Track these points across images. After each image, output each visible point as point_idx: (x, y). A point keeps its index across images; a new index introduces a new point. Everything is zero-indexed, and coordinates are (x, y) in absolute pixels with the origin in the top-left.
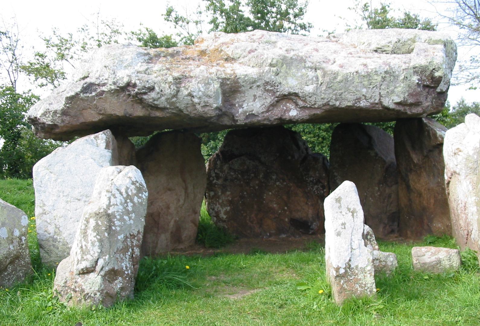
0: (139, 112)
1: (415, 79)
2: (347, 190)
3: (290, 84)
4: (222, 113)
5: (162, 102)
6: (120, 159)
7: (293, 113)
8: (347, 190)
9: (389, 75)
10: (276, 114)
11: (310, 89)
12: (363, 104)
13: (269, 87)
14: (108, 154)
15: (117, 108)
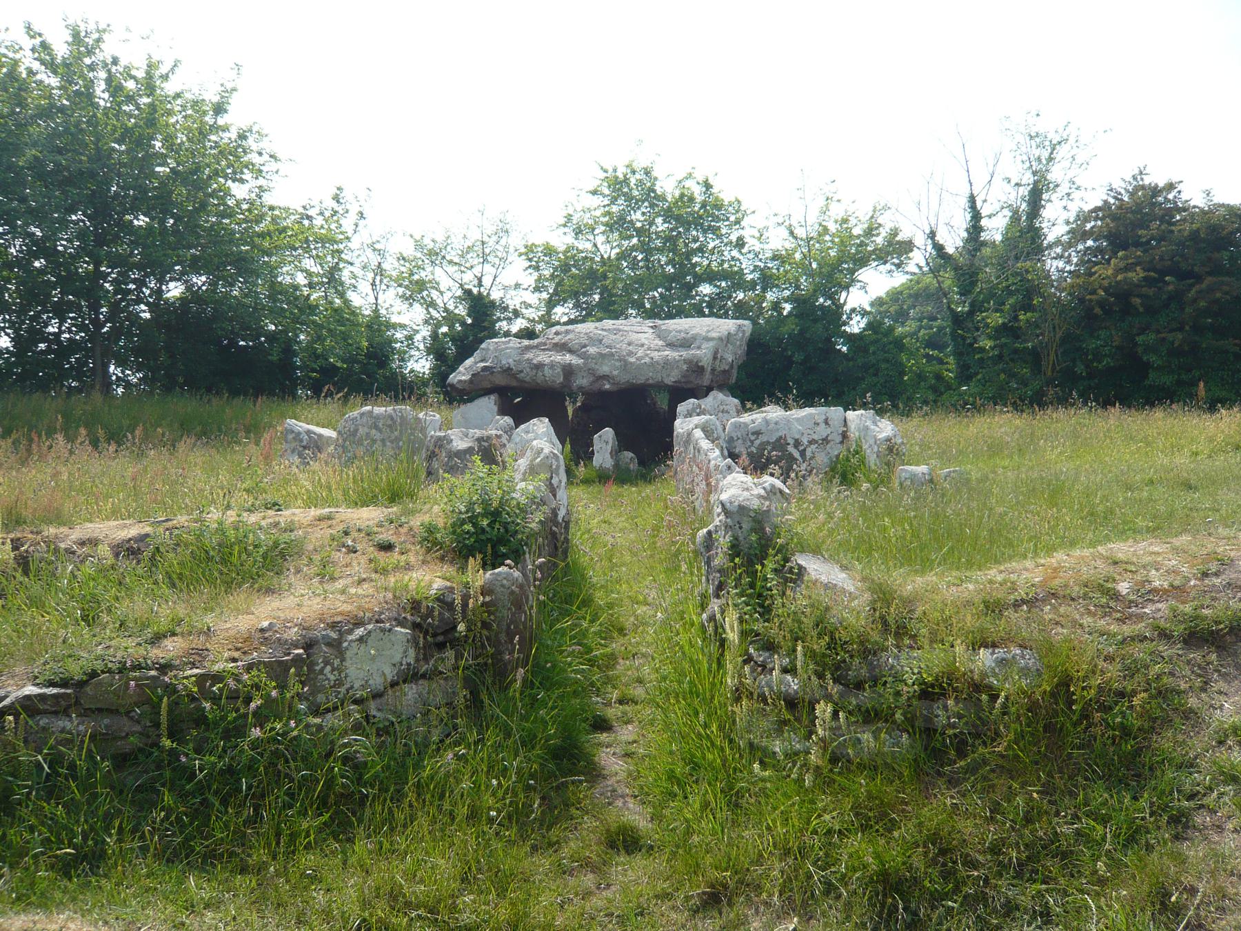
0: (514, 384)
1: (685, 367)
2: (608, 432)
3: (605, 369)
4: (563, 385)
5: (528, 379)
6: (503, 411)
7: (607, 386)
8: (608, 432)
9: (667, 363)
10: (597, 386)
11: (616, 373)
12: (651, 381)
13: (591, 372)
14: (495, 408)
15: (501, 381)
